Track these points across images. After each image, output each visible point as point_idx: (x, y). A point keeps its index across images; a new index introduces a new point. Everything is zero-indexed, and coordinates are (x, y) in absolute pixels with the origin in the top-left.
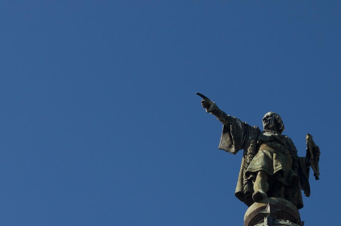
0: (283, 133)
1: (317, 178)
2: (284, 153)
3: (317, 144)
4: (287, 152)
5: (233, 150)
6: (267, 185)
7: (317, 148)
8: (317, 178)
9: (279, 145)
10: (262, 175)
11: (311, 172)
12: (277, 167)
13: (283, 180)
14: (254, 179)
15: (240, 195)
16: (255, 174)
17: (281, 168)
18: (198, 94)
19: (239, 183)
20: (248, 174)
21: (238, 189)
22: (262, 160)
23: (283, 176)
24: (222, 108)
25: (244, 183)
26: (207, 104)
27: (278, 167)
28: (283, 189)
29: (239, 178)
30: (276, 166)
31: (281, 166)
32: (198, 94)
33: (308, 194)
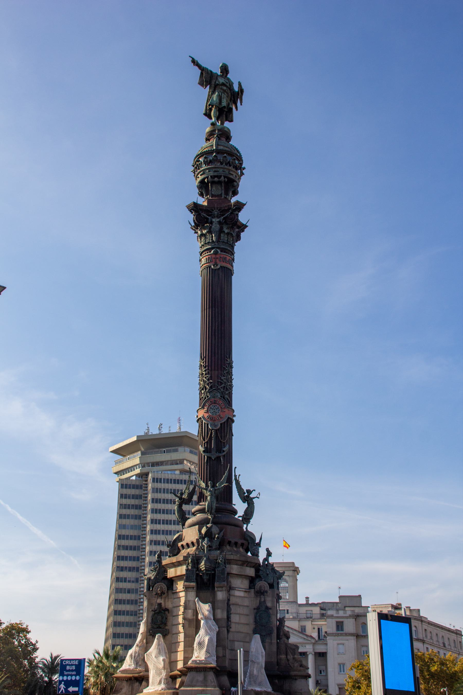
0: (229, 76)
1: (241, 105)
2: (227, 93)
3: (243, 87)
4: (229, 91)
6: (218, 113)
7: (243, 90)
8: (241, 105)
9: (225, 88)
10: (215, 108)
13: (226, 110)
18: (190, 56)
24: (200, 63)
26: (194, 61)
28: (225, 113)
32: (190, 56)
33: (237, 110)
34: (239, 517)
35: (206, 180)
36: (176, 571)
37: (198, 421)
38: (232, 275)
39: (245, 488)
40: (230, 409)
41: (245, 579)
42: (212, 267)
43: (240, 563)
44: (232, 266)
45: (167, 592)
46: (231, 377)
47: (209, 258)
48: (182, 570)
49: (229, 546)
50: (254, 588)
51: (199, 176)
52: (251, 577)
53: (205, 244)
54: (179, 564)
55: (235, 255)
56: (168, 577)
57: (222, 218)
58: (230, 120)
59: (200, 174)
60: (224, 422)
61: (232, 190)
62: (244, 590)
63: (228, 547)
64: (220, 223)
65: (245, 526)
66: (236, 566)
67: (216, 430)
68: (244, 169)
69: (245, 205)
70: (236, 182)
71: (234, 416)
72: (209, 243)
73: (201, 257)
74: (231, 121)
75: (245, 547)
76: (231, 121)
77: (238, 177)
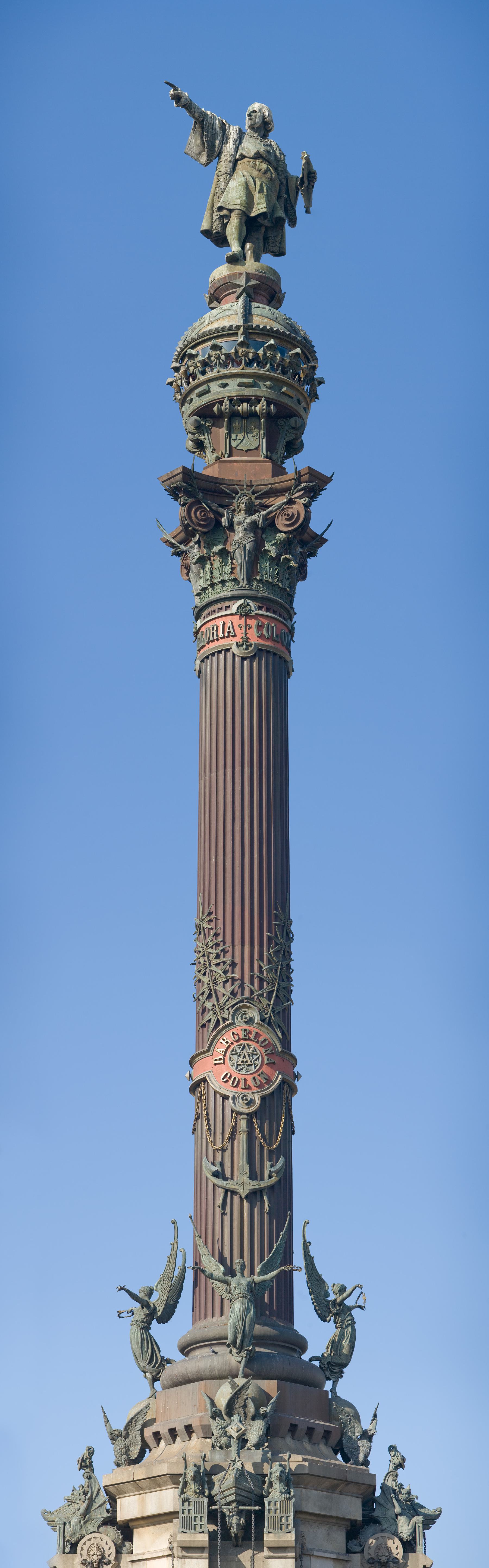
1: (308, 211)
5: (204, 159)
6: (244, 233)
8: (308, 211)
11: (301, 201)
12: (260, 206)
13: (266, 223)
14: (228, 217)
15: (207, 233)
16: (231, 211)
17: (265, 210)
19: (207, 214)
20: (221, 209)
21: (205, 226)
22: (242, 191)
23: (265, 218)
25: (215, 217)
27: (261, 206)
28: (263, 230)
29: (208, 207)
30: (259, 204)
31: (265, 205)
34: (313, 1359)
35: (215, 409)
36: (143, 1503)
37: (193, 1089)
38: (288, 675)
39: (331, 1277)
40: (286, 1056)
41: (335, 1528)
42: (234, 649)
43: (328, 1483)
44: (289, 651)
45: (118, 1558)
46: (288, 966)
47: (224, 624)
48: (166, 1499)
49: (293, 1437)
50: (362, 1552)
51: (193, 396)
52: (353, 1522)
53: (213, 585)
54: (155, 1482)
55: (295, 619)
56: (118, 1519)
57: (264, 513)
58: (276, 249)
59: (197, 391)
60: (273, 1093)
61: (288, 439)
62: (334, 1556)
63: (289, 1440)
64: (254, 526)
65: (328, 1385)
66: (315, 1492)
67: (250, 1116)
68: (321, 382)
69: (329, 480)
70: (301, 417)
71: (297, 1076)
72: (223, 582)
73: (199, 623)
74: (281, 253)
75: (334, 1440)
76: (281, 253)
77: (303, 404)
